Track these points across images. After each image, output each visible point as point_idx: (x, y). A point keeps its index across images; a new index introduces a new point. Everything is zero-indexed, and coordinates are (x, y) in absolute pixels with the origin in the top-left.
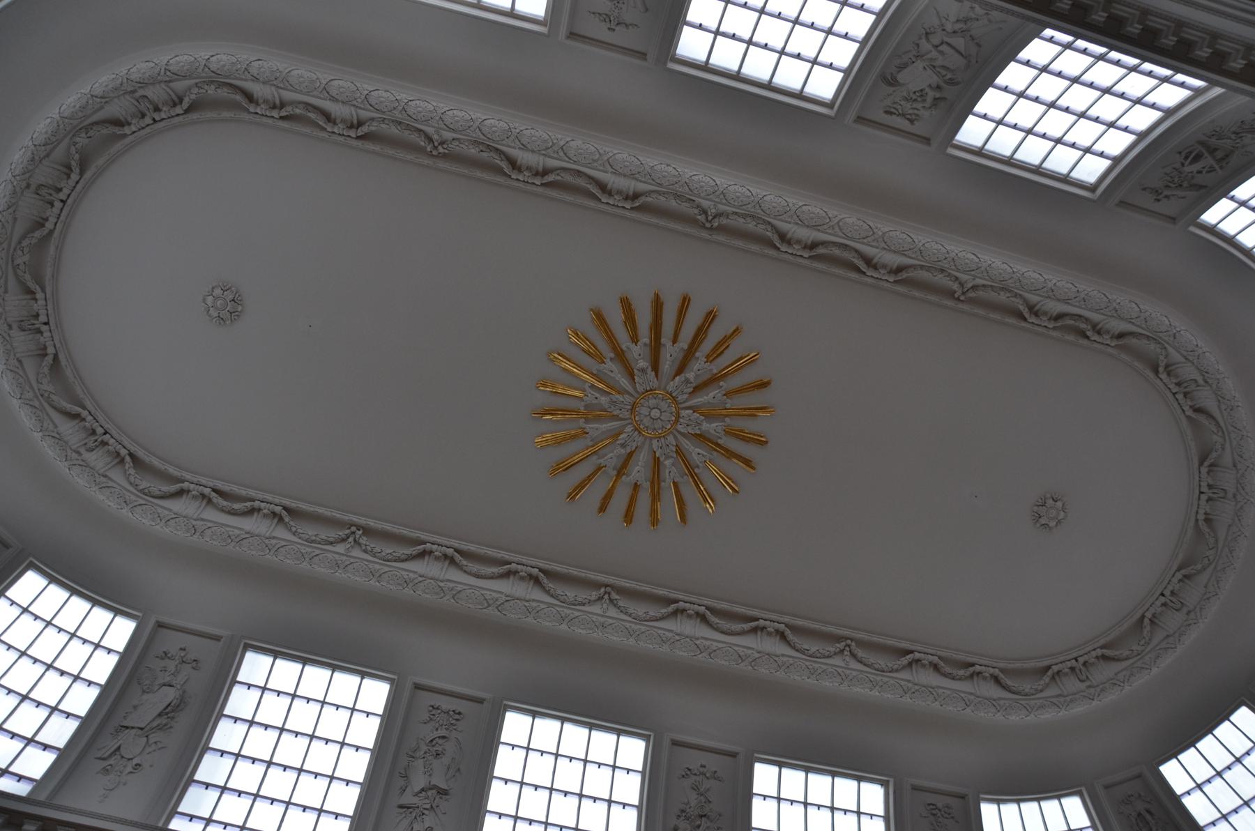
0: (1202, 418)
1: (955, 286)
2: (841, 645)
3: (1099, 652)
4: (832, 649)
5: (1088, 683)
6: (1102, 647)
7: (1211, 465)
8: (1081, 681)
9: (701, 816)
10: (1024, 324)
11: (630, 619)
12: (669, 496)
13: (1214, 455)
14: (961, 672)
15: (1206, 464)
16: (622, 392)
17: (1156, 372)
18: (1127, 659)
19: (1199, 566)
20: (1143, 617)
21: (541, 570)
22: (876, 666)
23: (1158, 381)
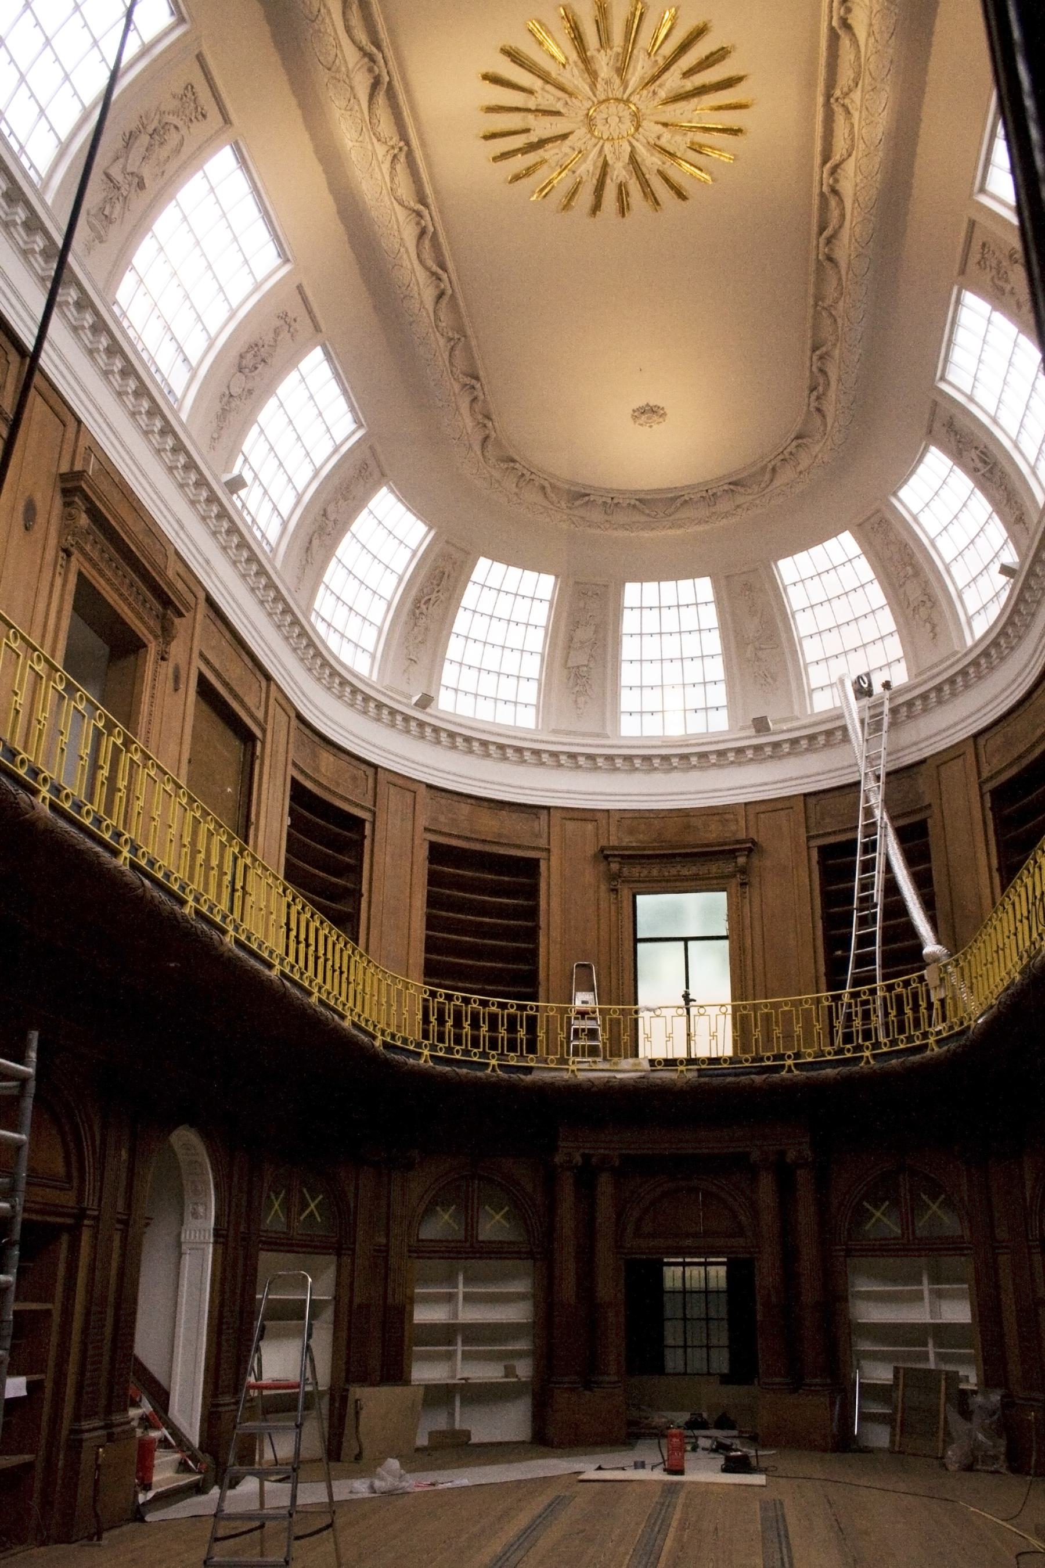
0: (767, 477)
1: (828, 302)
2: (457, 336)
3: (546, 484)
4: (450, 334)
5: (517, 490)
6: (551, 484)
7: (732, 491)
8: (517, 486)
9: (263, 361)
10: (809, 353)
11: (389, 185)
12: (532, 158)
13: (741, 490)
14: (480, 417)
15: (732, 487)
16: (625, 84)
17: (797, 438)
18: (552, 504)
19: (647, 511)
20: (588, 495)
21: (390, 83)
22: (454, 369)
23: (789, 441)
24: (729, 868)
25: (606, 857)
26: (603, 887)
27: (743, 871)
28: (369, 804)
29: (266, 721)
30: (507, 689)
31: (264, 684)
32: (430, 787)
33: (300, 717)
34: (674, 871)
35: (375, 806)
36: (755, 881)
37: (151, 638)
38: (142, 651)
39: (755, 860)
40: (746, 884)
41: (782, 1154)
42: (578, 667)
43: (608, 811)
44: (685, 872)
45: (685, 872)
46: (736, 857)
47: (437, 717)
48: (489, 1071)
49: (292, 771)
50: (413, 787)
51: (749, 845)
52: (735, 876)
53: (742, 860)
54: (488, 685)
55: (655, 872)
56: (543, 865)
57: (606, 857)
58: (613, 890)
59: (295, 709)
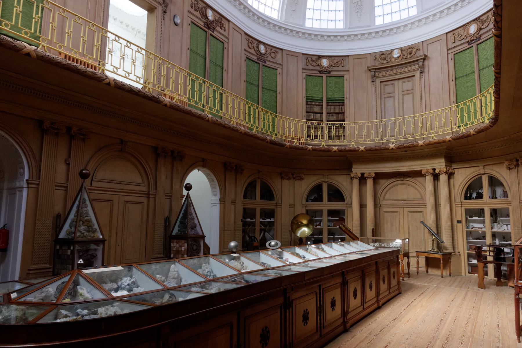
24: (417, 66)
25: (370, 70)
26: (370, 81)
27: (423, 66)
28: (280, 62)
29: (229, 36)
30: (332, 16)
31: (227, 22)
32: (303, 54)
33: (246, 34)
34: (395, 72)
35: (282, 63)
36: (426, 70)
37: (160, 6)
38: (156, 11)
39: (426, 63)
40: (423, 72)
41: (434, 170)
42: (357, 2)
43: (370, 53)
44: (399, 71)
45: (399, 71)
46: (418, 63)
47: (305, 29)
48: (321, 146)
49: (243, 52)
50: (297, 55)
51: (423, 57)
52: (417, 70)
53: (421, 64)
54: (324, 15)
55: (388, 73)
56: (346, 77)
57: (370, 70)
58: (372, 82)
59: (244, 31)
